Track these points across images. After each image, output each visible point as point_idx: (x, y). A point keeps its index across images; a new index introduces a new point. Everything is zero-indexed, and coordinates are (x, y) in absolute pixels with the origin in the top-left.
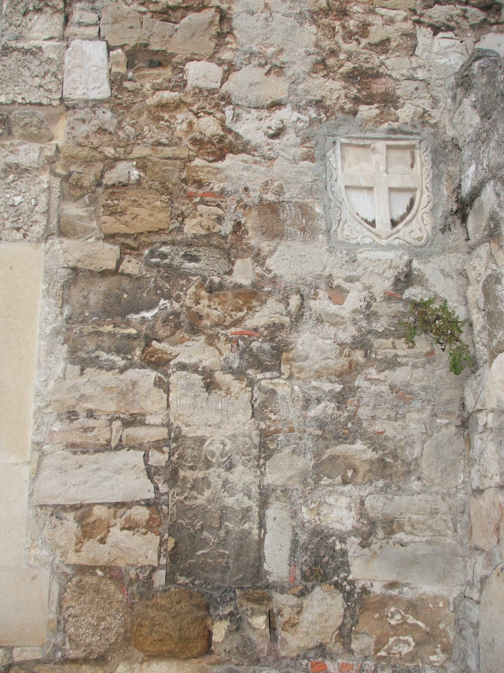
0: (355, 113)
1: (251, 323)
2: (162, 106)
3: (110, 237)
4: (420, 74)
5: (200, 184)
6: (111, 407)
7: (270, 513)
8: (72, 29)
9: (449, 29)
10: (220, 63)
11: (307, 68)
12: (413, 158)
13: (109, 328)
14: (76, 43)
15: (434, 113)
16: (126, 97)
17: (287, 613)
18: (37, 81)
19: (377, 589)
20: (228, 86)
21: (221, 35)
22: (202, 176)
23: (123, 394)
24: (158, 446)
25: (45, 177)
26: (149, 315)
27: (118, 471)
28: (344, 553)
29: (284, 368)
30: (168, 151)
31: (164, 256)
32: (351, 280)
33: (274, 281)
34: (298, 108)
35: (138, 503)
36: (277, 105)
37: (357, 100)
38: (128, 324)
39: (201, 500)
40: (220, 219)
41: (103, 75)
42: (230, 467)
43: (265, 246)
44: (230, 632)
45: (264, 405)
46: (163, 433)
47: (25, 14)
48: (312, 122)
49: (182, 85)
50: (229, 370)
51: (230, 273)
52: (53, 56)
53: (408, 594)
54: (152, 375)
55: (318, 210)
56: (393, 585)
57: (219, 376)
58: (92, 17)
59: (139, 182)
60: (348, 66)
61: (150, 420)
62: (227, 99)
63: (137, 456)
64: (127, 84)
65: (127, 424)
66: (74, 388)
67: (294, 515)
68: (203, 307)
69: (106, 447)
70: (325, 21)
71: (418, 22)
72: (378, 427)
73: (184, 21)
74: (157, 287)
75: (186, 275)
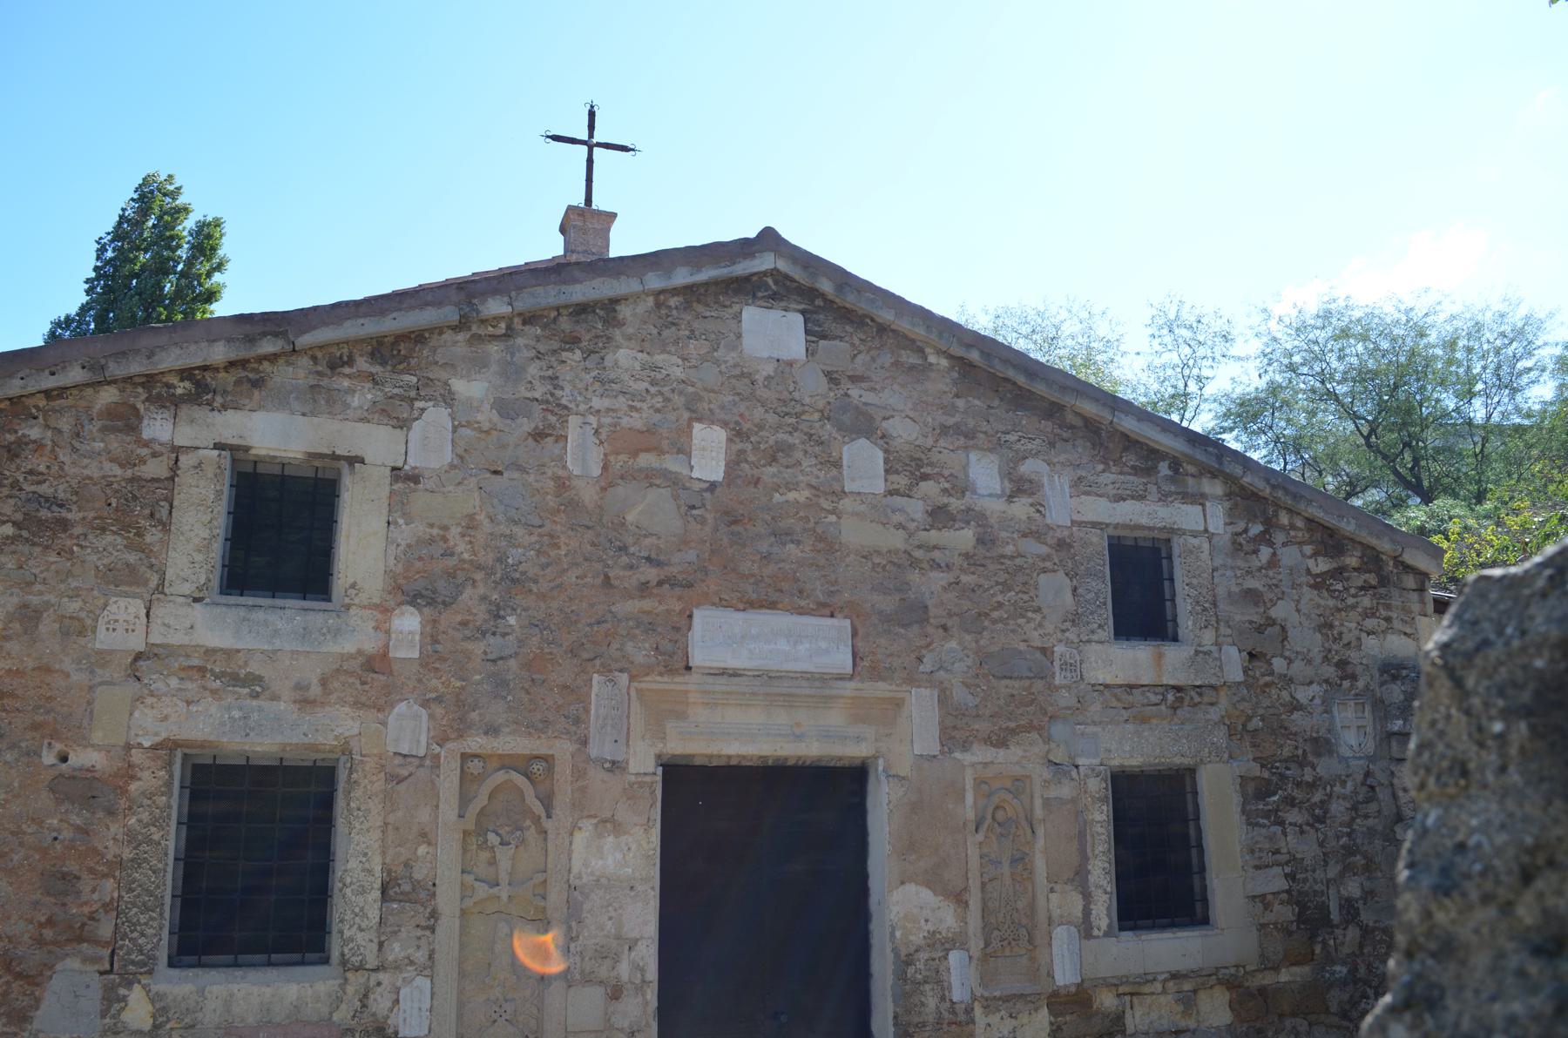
0: (1341, 685)
1: (1313, 801)
2: (1267, 685)
3: (1255, 759)
4: (1364, 661)
5: (1286, 729)
6: (1267, 846)
7: (1330, 892)
8: (1220, 639)
9: (1374, 633)
10: (1285, 658)
11: (1320, 661)
12: (1364, 708)
13: (1261, 807)
14: (1225, 648)
15: (1371, 683)
16: (1251, 680)
17: (1340, 937)
18: (1212, 671)
19: (1371, 924)
20: (1290, 673)
21: (1283, 641)
22: (1286, 724)
23: (1271, 839)
24: (1287, 863)
25: (1222, 727)
26: (1276, 798)
27: (1274, 877)
28: (1358, 908)
29: (1328, 821)
30: (1271, 711)
31: (1277, 768)
32: (1347, 776)
33: (1320, 778)
34: (1319, 684)
35: (1283, 892)
36: (1311, 683)
37: (1342, 679)
38: (1267, 804)
39: (1306, 888)
40: (1296, 748)
41: (1240, 667)
42: (1314, 871)
43: (1316, 761)
44: (1322, 949)
45: (1323, 841)
46: (1287, 857)
47: (1201, 628)
48: (1326, 691)
49: (1272, 673)
50: (1308, 824)
51: (1303, 775)
52: (1217, 656)
53: (1382, 925)
54: (1280, 828)
55: (1333, 741)
56: (1376, 922)
57: (1306, 828)
58: (1229, 631)
59: (1262, 729)
60: (1337, 658)
61: (1282, 851)
62: (1291, 680)
63: (1278, 870)
64: (1250, 672)
65: (1273, 854)
66: (1253, 838)
67: (1339, 891)
68: (1295, 794)
69: (1267, 866)
70: (1324, 631)
71: (1361, 630)
72: (1365, 848)
73: (1266, 632)
74: (1277, 784)
75: (1287, 778)
